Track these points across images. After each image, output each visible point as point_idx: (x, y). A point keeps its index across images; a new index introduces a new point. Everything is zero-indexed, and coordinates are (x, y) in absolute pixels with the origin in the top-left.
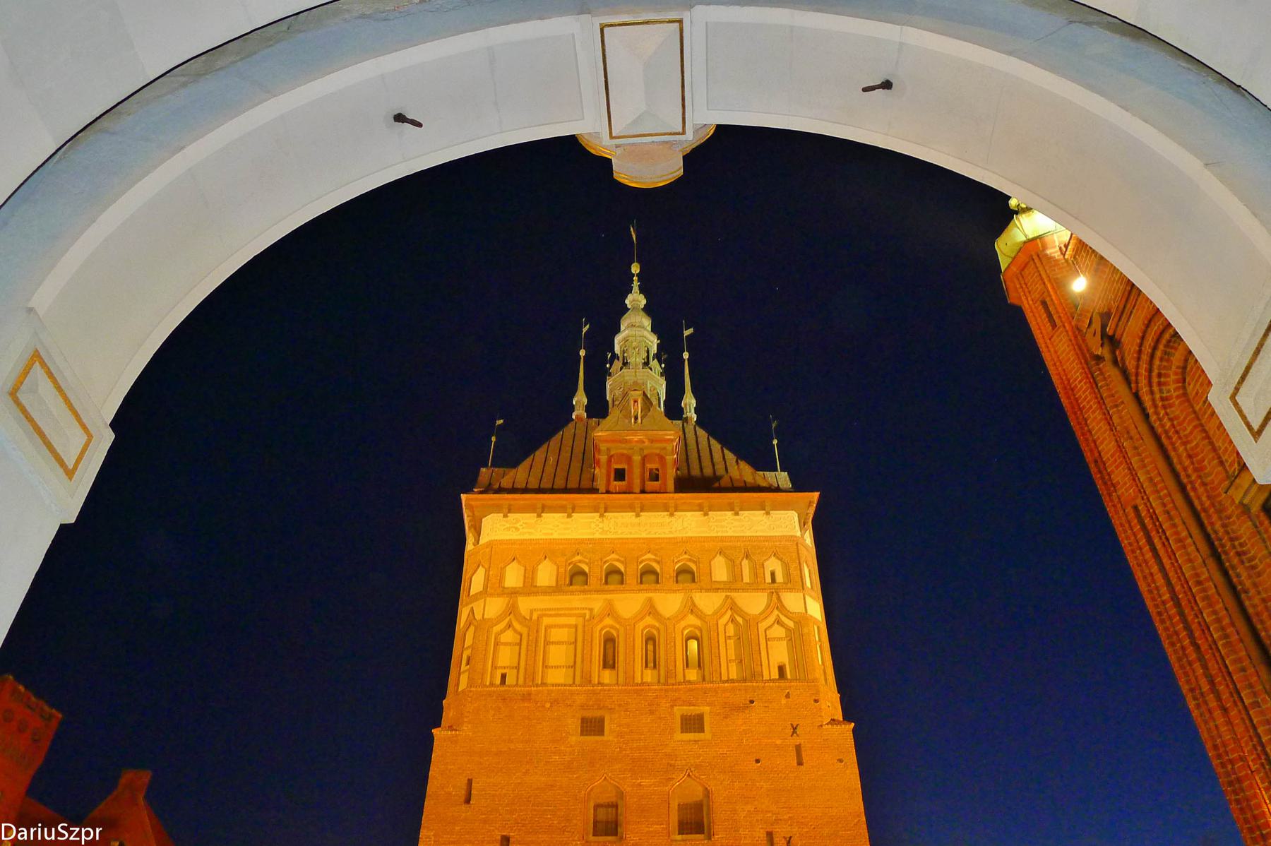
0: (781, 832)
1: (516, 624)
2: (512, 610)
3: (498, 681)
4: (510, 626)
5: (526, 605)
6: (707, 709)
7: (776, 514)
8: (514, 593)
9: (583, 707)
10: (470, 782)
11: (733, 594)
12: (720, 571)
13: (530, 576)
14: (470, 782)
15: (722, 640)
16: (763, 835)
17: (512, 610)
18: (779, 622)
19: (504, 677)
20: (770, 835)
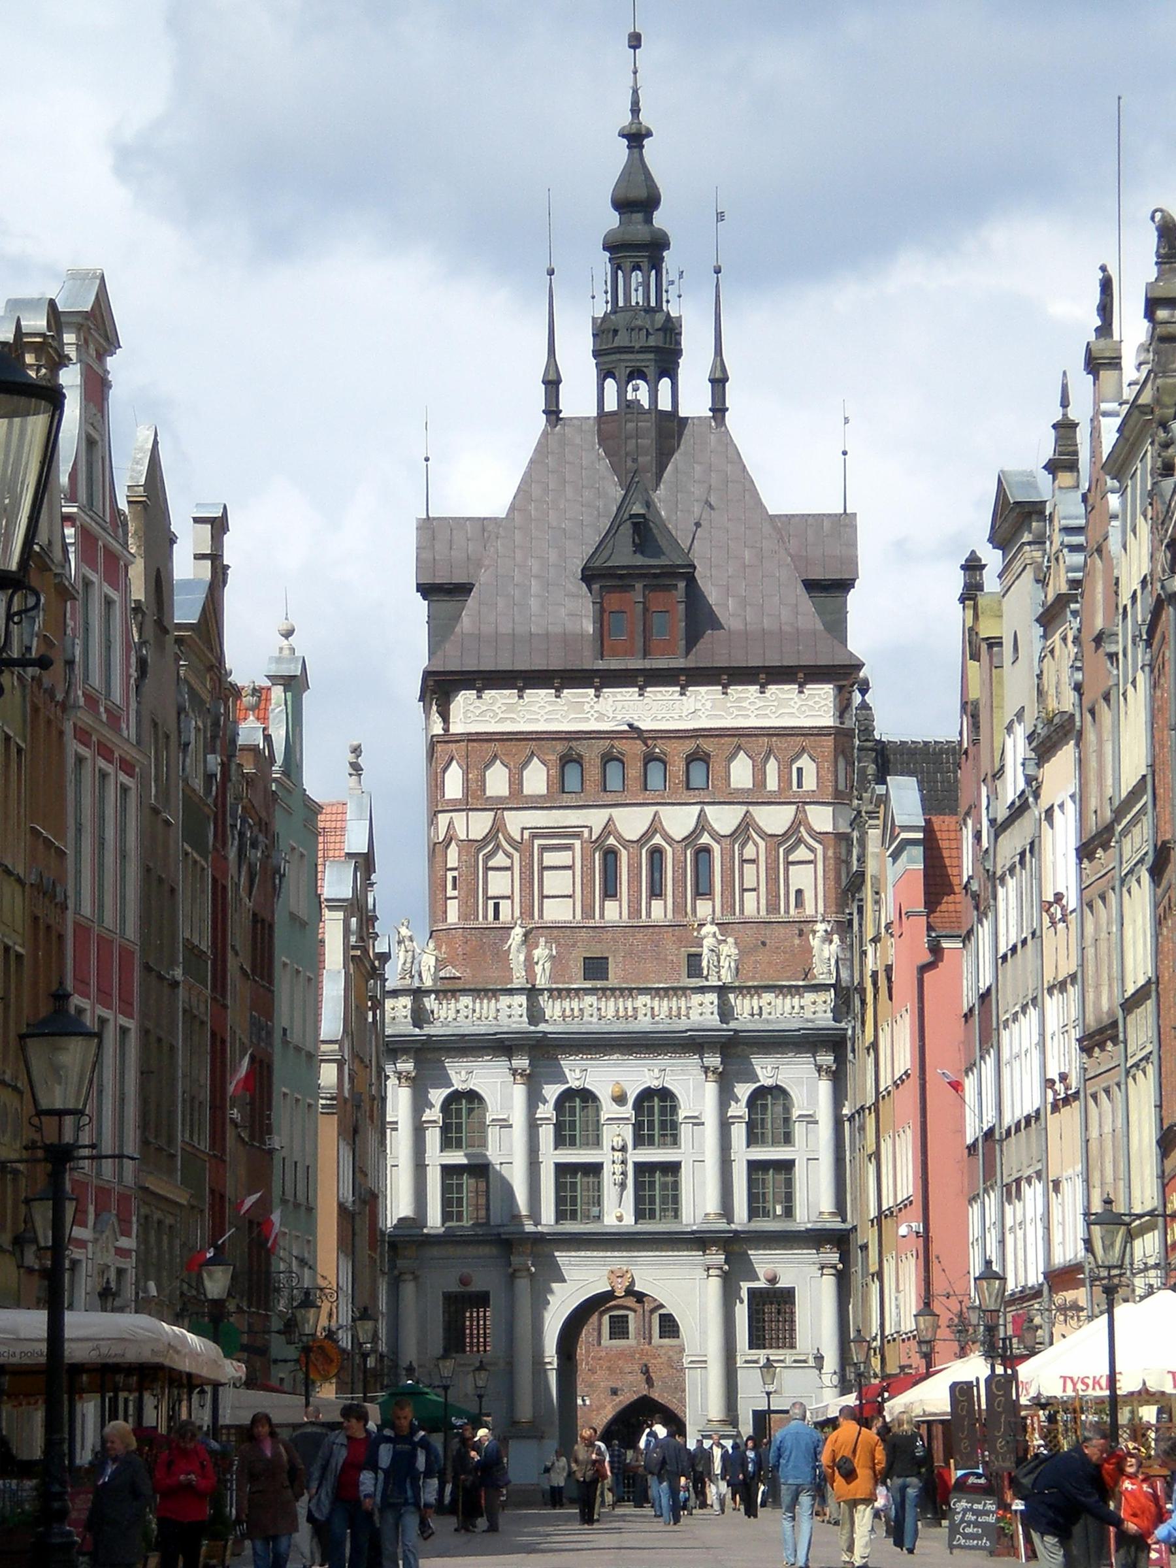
2: (498, 828)
5: (516, 822)
7: (811, 689)
8: (498, 806)
11: (751, 808)
12: (741, 773)
13: (516, 782)
17: (498, 828)
18: (800, 841)
19: (497, 906)
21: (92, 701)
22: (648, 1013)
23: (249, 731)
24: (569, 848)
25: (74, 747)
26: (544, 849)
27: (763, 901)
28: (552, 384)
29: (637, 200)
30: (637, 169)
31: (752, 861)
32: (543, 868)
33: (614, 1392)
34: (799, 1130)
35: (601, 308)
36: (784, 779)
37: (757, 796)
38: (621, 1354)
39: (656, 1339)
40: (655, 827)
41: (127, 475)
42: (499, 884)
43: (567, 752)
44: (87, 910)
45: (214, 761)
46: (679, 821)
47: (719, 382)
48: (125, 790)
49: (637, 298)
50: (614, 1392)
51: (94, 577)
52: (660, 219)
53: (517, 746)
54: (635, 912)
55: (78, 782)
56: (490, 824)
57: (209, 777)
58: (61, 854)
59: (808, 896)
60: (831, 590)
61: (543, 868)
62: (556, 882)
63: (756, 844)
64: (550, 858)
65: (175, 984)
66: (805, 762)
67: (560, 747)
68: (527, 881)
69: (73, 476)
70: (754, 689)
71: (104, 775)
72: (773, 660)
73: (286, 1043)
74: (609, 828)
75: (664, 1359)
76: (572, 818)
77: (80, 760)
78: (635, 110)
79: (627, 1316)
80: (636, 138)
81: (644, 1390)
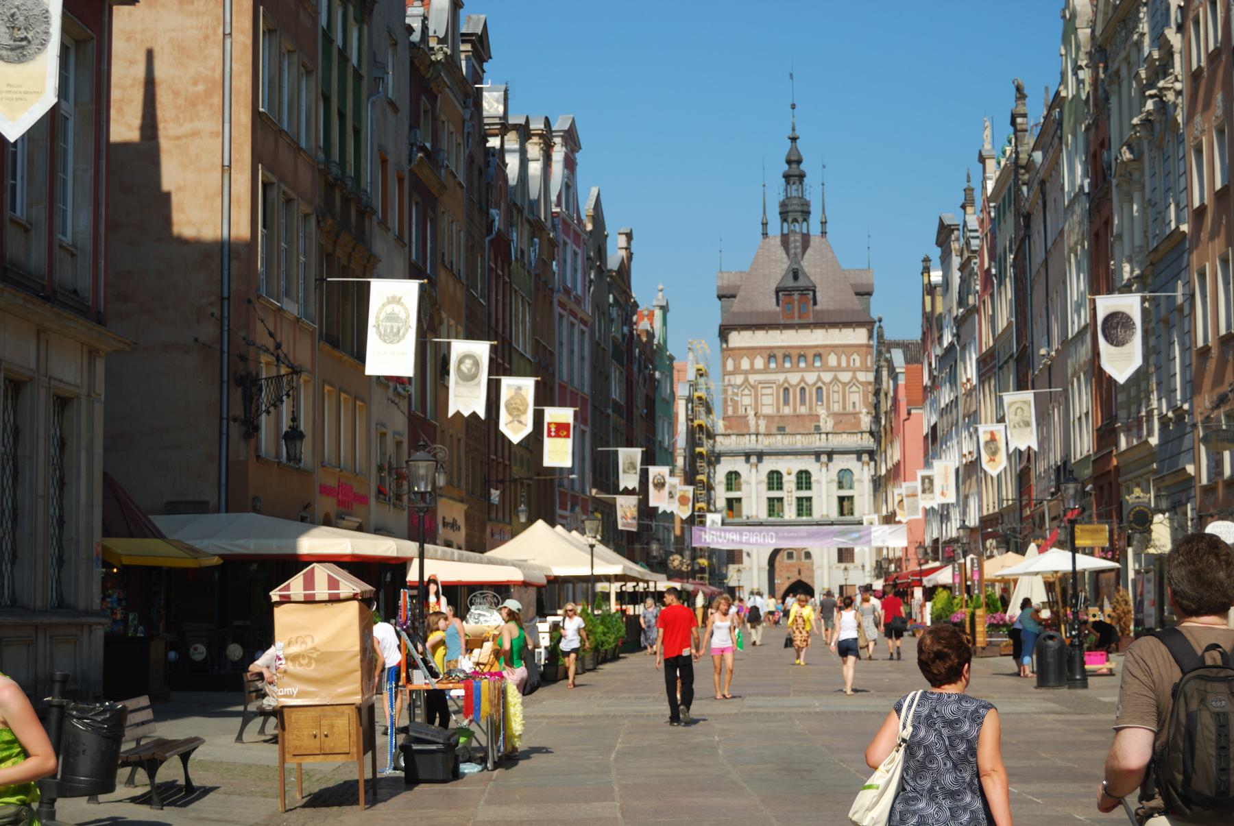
2: (746, 380)
5: (753, 378)
8: (746, 373)
12: (832, 360)
13: (752, 364)
17: (746, 380)
21: (567, 291)
22: (800, 442)
23: (644, 325)
25: (558, 310)
28: (765, 224)
29: (794, 161)
30: (794, 150)
34: (856, 485)
35: (782, 197)
36: (848, 362)
37: (839, 368)
38: (792, 565)
40: (803, 380)
41: (587, 207)
42: (747, 401)
43: (771, 354)
44: (565, 378)
45: (626, 329)
46: (811, 378)
47: (824, 223)
48: (583, 332)
49: (794, 194)
51: (568, 241)
52: (802, 167)
53: (751, 351)
54: (795, 410)
55: (560, 325)
57: (624, 336)
58: (552, 354)
60: (865, 293)
62: (767, 400)
64: (764, 391)
65: (608, 416)
66: (855, 356)
67: (768, 352)
69: (559, 197)
70: (837, 331)
71: (573, 325)
72: (844, 320)
73: (661, 447)
74: (786, 381)
76: (772, 377)
77: (561, 316)
78: (794, 130)
80: (794, 139)
81: (799, 578)
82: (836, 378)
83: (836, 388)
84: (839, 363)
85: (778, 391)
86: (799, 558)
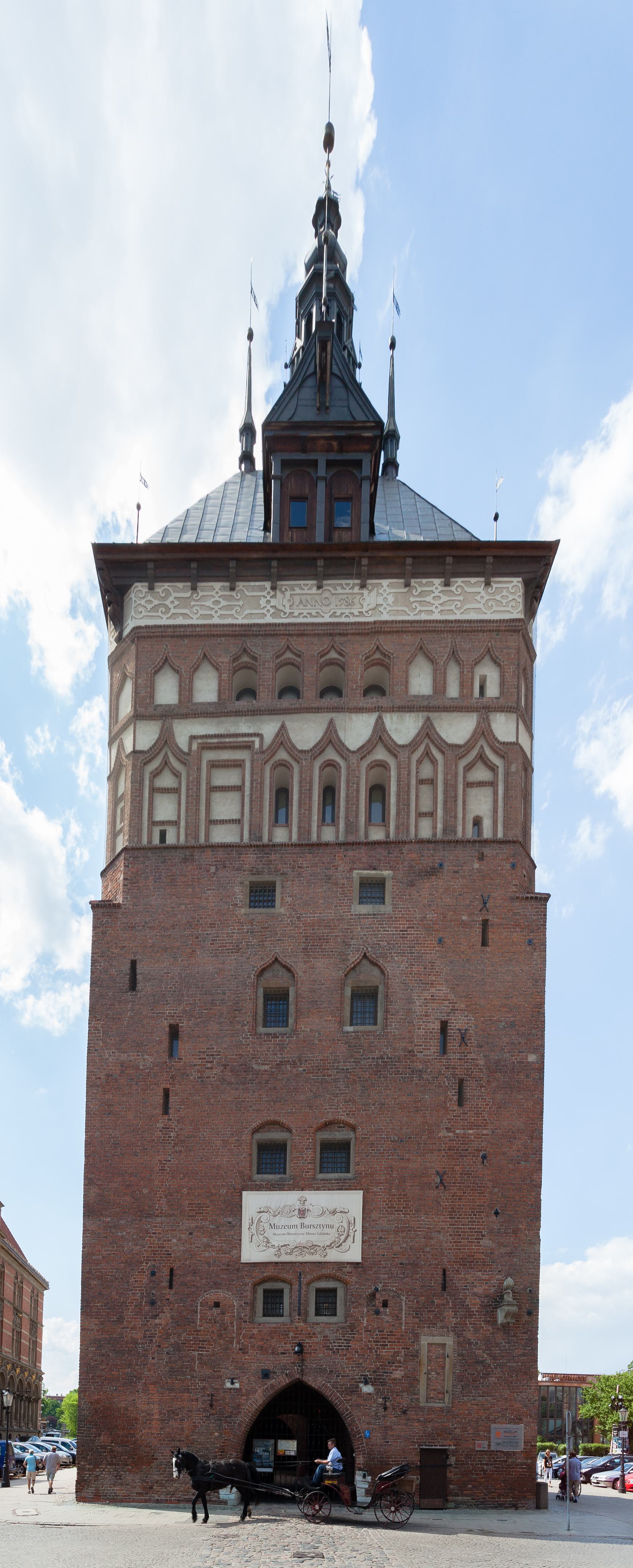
0: (457, 1023)
1: (172, 760)
2: (166, 740)
3: (156, 841)
4: (166, 763)
6: (386, 873)
9: (254, 872)
10: (134, 964)
13: (186, 690)
14: (134, 964)
15: (413, 782)
16: (437, 1026)
17: (166, 740)
18: (481, 757)
20: (444, 1026)
24: (238, 764)
26: (214, 765)
27: (440, 826)
31: (432, 782)
32: (212, 789)
33: (266, 1375)
39: (312, 1318)
50: (266, 1375)
56: (156, 736)
59: (487, 824)
61: (212, 789)
63: (434, 762)
68: (193, 800)
75: (319, 1338)
79: (281, 1291)
82: (428, 733)
83: (426, 771)
84: (440, 686)
85: (257, 785)
86: (302, 1313)
